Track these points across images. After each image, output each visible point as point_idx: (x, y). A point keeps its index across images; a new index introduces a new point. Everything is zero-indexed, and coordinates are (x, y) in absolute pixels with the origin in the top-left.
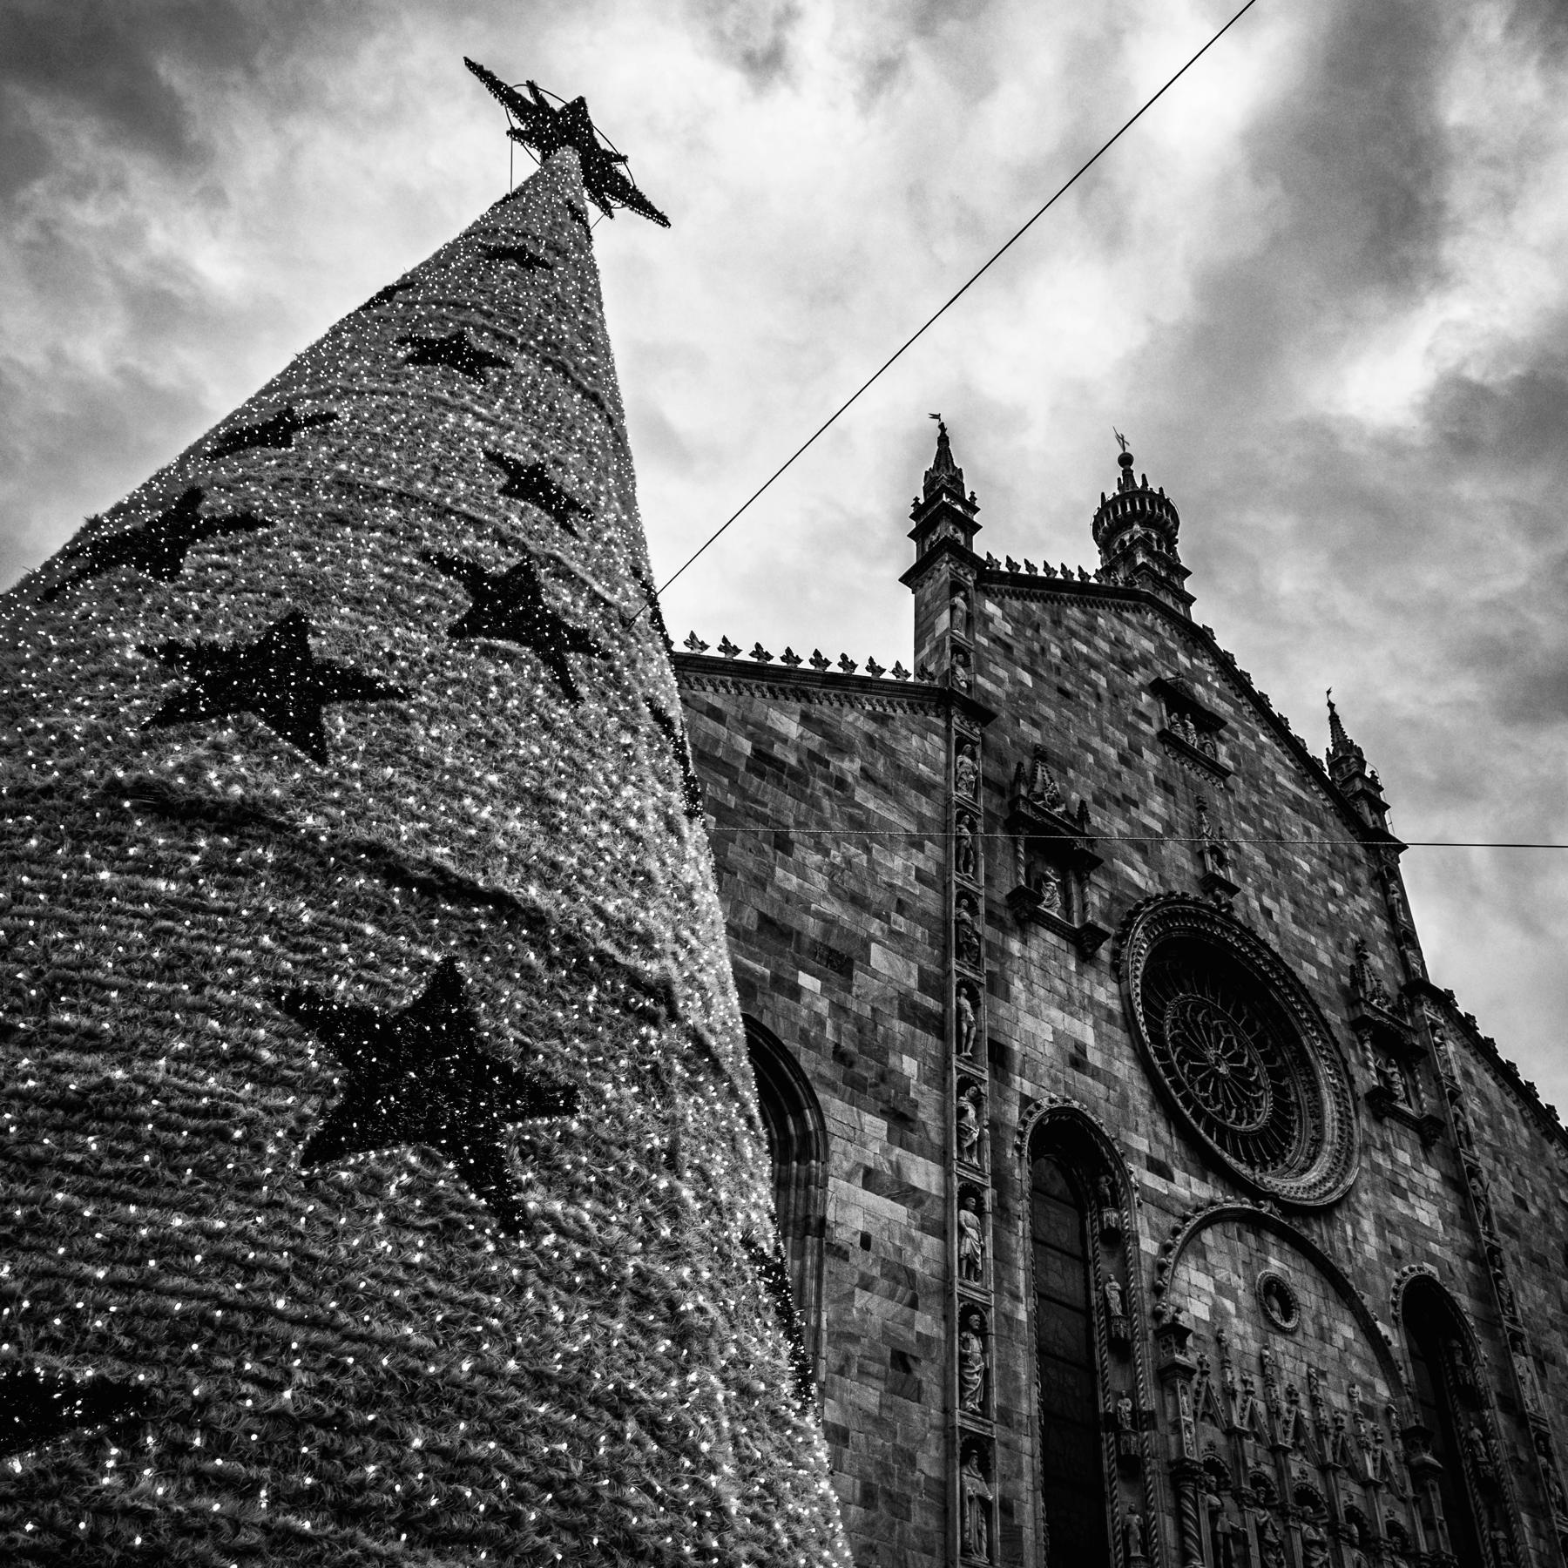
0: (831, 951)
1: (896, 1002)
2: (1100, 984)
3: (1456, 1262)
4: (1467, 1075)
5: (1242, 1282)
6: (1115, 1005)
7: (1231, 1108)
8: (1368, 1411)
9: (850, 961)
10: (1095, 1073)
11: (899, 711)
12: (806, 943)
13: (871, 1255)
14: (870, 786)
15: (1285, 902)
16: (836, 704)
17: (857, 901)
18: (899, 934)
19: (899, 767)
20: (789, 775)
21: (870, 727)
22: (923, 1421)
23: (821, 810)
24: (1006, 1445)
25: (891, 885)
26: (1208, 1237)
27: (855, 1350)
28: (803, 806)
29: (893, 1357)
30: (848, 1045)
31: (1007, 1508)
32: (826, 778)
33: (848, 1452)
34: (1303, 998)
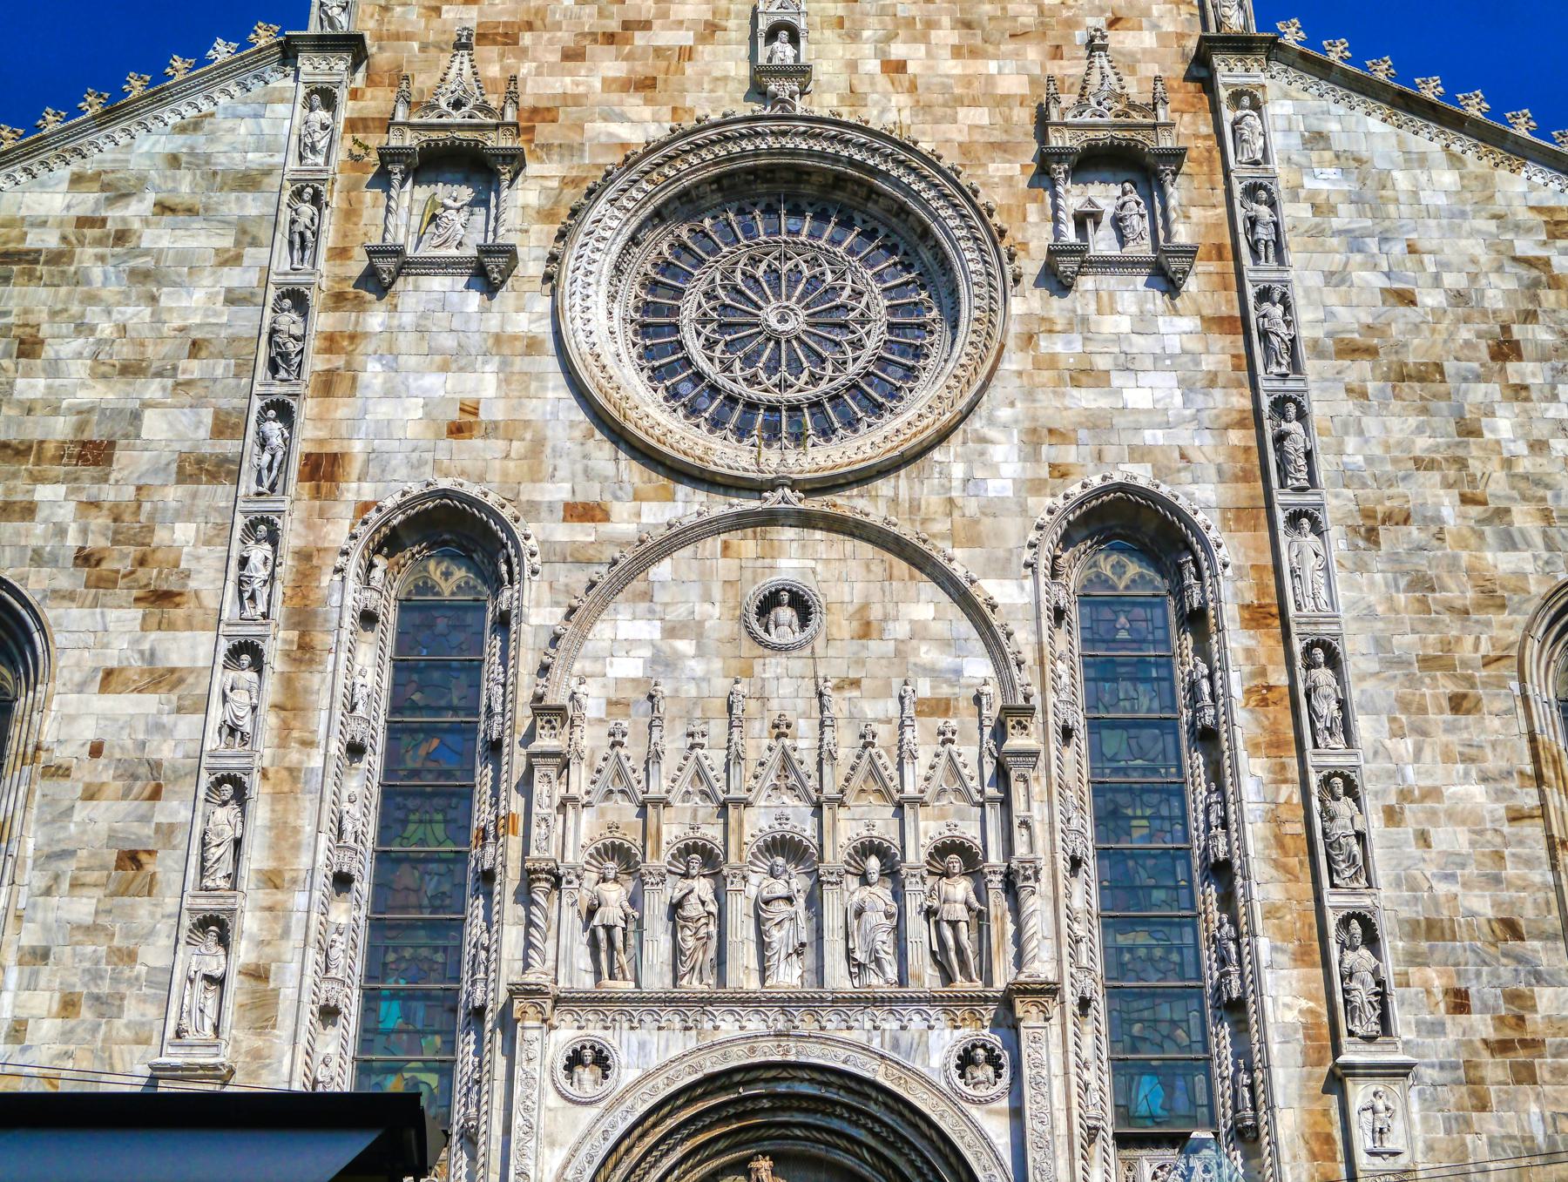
0: (84, 444)
1: (174, 467)
2: (519, 310)
3: (1202, 445)
4: (1317, 139)
5: (716, 611)
6: (544, 329)
7: (797, 369)
8: (941, 707)
9: (112, 444)
10: (491, 430)
11: (223, 100)
12: (50, 449)
13: (102, 761)
14: (168, 218)
15: (946, 35)
16: (124, 140)
17: (130, 370)
18: (189, 383)
19: (215, 173)
20: (47, 263)
21: (178, 143)
22: (152, 915)
23: (88, 282)
24: (270, 909)
25: (181, 330)
26: (662, 570)
27: (68, 867)
28: (63, 290)
29: (119, 858)
30: (96, 542)
31: (258, 974)
32: (99, 242)
33: (45, 972)
34: (927, 171)
